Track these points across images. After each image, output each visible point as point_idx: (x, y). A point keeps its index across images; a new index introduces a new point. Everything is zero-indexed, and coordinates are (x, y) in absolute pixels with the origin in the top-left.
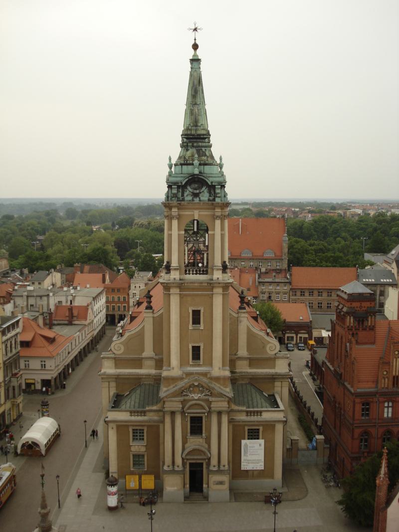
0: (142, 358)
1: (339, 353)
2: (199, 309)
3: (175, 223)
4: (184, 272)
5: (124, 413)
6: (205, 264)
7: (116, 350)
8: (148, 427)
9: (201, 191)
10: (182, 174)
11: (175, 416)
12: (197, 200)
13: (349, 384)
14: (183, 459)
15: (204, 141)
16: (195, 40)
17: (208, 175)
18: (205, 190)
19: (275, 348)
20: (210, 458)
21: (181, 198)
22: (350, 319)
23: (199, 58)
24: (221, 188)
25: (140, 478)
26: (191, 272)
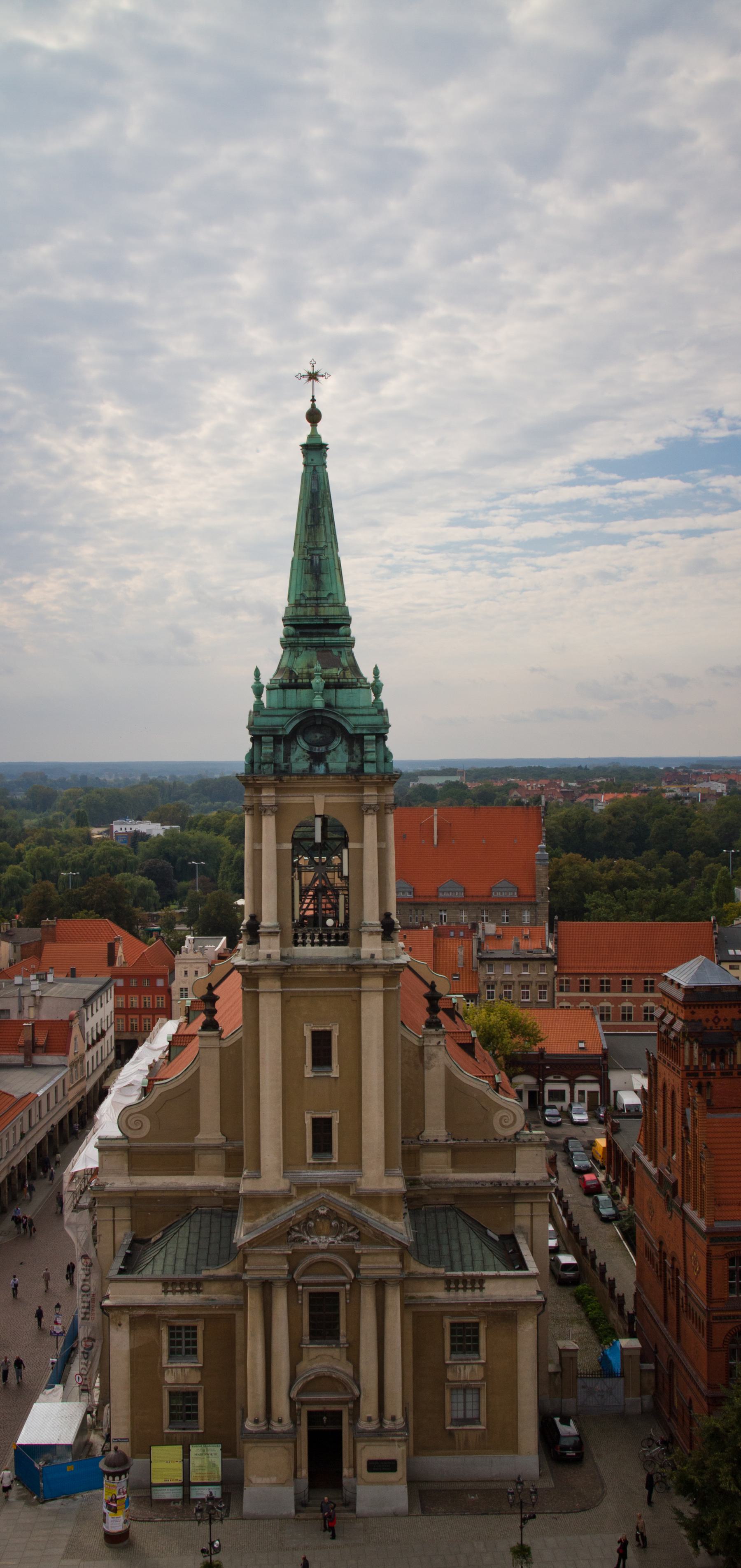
0: (194, 1148)
1: (669, 1132)
2: (328, 1029)
3: (269, 824)
4: (291, 939)
5: (150, 1286)
6: (342, 919)
7: (130, 1128)
8: (208, 1319)
9: (331, 748)
10: (284, 708)
12: (321, 769)
13: (695, 1209)
14: (292, 1402)
15: (335, 631)
16: (313, 400)
17: (345, 711)
18: (339, 745)
19: (515, 1121)
20: (359, 1398)
21: (283, 765)
22: (691, 1048)
23: (324, 441)
24: (377, 741)
25: (186, 1454)
26: (308, 940)
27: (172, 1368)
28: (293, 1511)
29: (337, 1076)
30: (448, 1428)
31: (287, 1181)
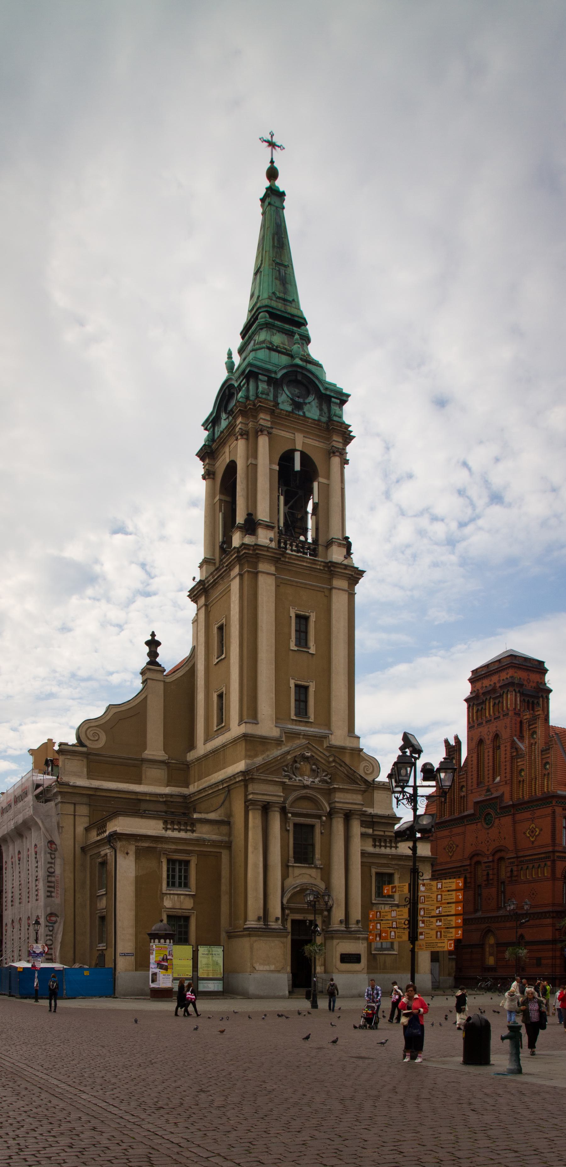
2: (307, 614)
27: (170, 894)
29: (314, 653)
31: (278, 730)
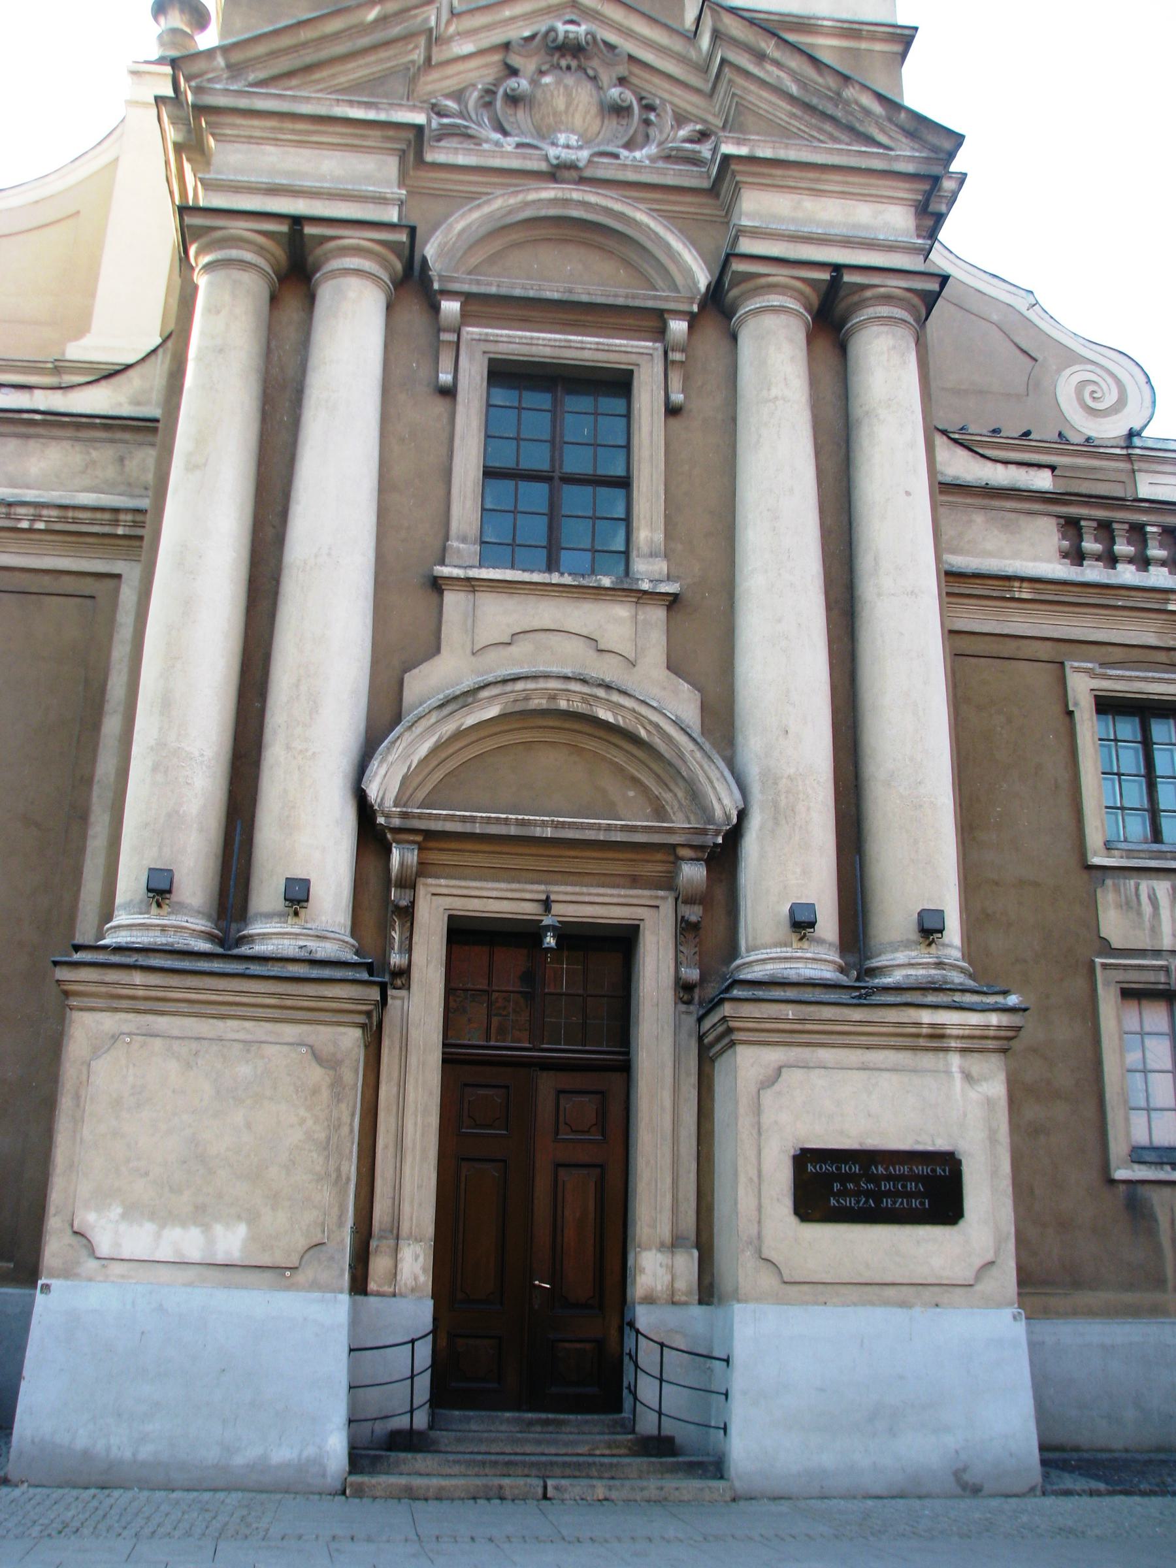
11: (311, 299)
19: (1121, 403)
20: (735, 834)
28: (335, 1445)
30: (1120, 1174)
